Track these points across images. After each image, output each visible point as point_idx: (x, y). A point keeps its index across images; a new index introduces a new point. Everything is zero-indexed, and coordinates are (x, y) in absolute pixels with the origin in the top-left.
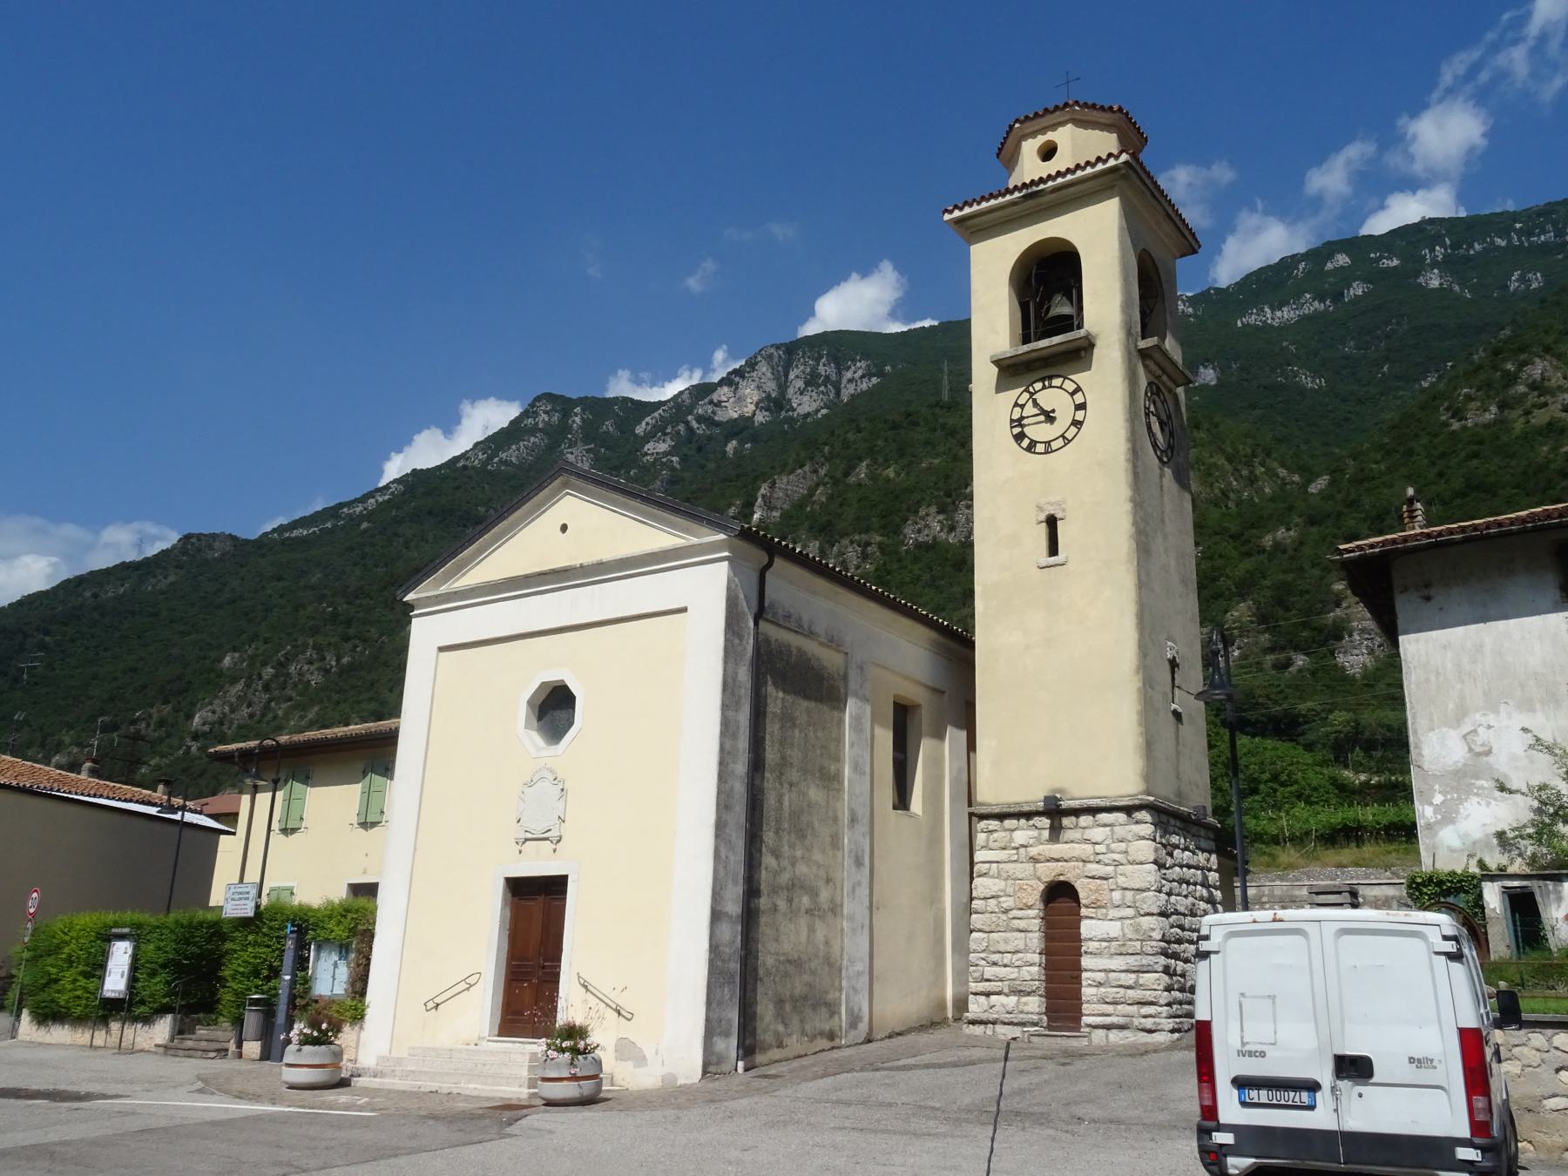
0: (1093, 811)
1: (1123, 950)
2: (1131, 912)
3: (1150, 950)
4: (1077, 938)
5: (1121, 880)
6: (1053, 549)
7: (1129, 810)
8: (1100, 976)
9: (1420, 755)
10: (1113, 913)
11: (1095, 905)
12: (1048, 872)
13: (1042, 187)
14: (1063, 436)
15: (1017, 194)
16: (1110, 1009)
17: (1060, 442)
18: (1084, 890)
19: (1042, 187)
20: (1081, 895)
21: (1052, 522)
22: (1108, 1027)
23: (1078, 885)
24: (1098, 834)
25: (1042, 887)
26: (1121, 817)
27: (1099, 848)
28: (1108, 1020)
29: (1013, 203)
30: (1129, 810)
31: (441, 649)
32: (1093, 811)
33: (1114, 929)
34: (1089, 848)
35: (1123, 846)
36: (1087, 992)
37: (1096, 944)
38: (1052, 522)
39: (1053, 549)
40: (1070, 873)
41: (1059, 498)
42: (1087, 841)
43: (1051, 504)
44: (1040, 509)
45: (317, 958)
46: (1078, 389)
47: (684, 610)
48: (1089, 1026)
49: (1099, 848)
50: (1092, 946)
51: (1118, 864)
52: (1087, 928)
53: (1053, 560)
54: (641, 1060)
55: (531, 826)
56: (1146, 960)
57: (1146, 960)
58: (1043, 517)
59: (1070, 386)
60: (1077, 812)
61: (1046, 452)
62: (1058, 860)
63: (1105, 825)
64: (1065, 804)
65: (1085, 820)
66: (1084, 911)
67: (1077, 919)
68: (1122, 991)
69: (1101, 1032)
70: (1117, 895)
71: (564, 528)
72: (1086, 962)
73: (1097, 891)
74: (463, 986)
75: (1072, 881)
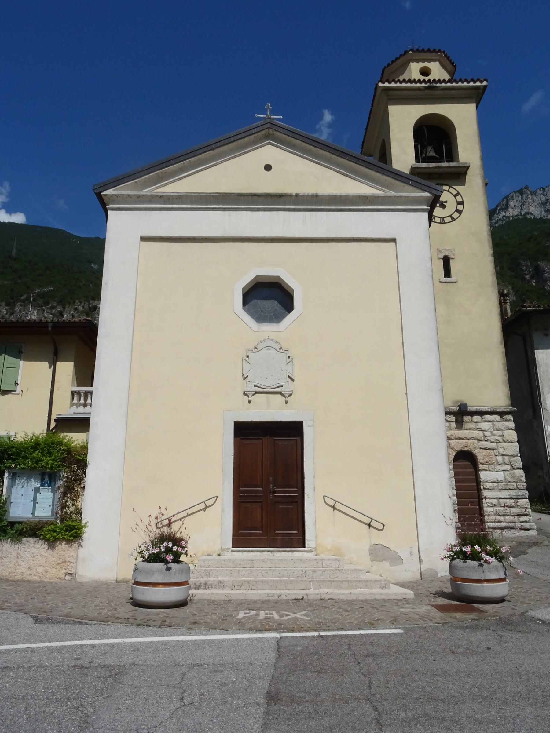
0: (481, 413)
1: (507, 487)
2: (509, 467)
3: (522, 487)
4: (478, 482)
5: (501, 450)
6: (447, 273)
7: (501, 414)
8: (495, 501)
9: (545, 403)
10: (498, 468)
11: (488, 463)
12: (458, 445)
13: (438, 85)
14: (451, 216)
15: (423, 85)
16: (502, 518)
17: (449, 219)
18: (480, 455)
19: (438, 85)
20: (480, 458)
21: (446, 261)
22: (502, 529)
23: (476, 452)
24: (485, 426)
25: (454, 453)
26: (497, 417)
27: (486, 433)
28: (503, 525)
29: (419, 89)
30: (501, 414)
31: (143, 239)
32: (481, 413)
33: (500, 476)
34: (481, 433)
35: (500, 433)
36: (487, 510)
37: (491, 484)
38: (446, 261)
39: (447, 273)
40: (472, 446)
41: (451, 248)
42: (478, 429)
43: (445, 249)
44: (441, 252)
45: (11, 486)
46: (458, 194)
47: (394, 240)
48: (489, 528)
49: (486, 433)
50: (488, 485)
51: (498, 442)
52: (484, 475)
53: (448, 279)
54: (397, 560)
55: (262, 383)
56: (520, 493)
57: (520, 493)
58: (441, 256)
59: (455, 192)
60: (472, 414)
61: (441, 223)
62: (463, 439)
63: (489, 421)
64: (470, 409)
65: (476, 418)
66: (481, 467)
67: (477, 471)
68: (508, 509)
69: (499, 531)
70: (500, 458)
71: (268, 168)
72: (485, 493)
73: (488, 456)
74: (203, 506)
75: (473, 449)
